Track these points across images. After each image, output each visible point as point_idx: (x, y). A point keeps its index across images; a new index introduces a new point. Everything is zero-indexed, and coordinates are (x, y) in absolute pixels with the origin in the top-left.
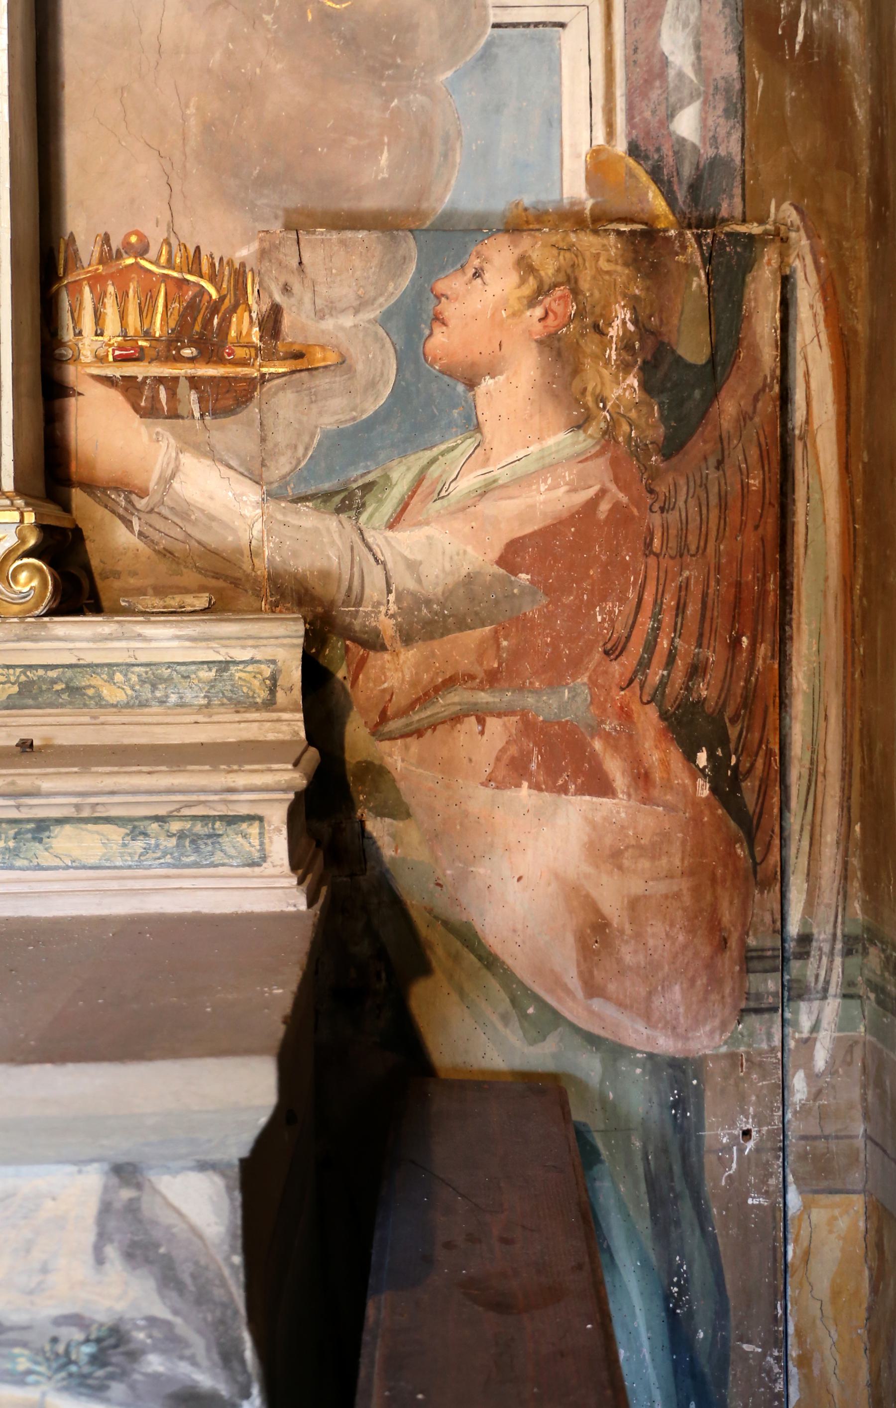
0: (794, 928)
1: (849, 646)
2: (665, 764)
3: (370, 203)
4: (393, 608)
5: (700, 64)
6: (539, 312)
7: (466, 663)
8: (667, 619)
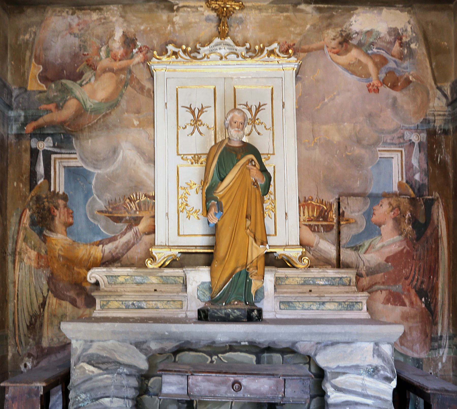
0: (439, 335)
1: (449, 279)
2: (416, 301)
3: (356, 191)
4: (365, 269)
5: (420, 166)
6: (393, 213)
7: (378, 280)
8: (417, 272)
